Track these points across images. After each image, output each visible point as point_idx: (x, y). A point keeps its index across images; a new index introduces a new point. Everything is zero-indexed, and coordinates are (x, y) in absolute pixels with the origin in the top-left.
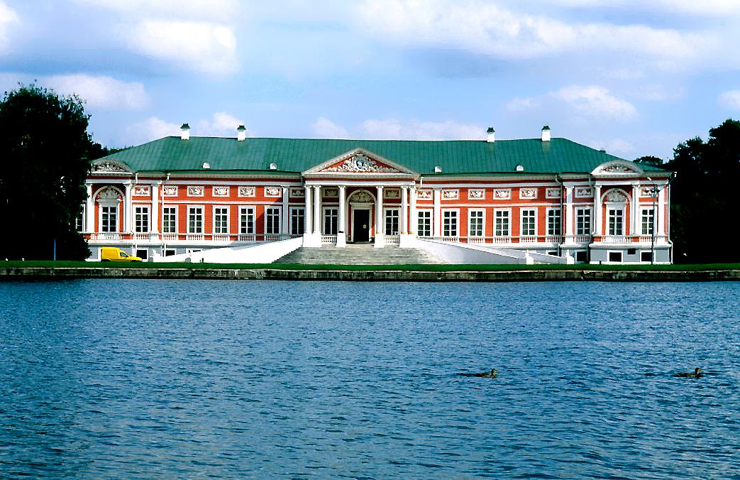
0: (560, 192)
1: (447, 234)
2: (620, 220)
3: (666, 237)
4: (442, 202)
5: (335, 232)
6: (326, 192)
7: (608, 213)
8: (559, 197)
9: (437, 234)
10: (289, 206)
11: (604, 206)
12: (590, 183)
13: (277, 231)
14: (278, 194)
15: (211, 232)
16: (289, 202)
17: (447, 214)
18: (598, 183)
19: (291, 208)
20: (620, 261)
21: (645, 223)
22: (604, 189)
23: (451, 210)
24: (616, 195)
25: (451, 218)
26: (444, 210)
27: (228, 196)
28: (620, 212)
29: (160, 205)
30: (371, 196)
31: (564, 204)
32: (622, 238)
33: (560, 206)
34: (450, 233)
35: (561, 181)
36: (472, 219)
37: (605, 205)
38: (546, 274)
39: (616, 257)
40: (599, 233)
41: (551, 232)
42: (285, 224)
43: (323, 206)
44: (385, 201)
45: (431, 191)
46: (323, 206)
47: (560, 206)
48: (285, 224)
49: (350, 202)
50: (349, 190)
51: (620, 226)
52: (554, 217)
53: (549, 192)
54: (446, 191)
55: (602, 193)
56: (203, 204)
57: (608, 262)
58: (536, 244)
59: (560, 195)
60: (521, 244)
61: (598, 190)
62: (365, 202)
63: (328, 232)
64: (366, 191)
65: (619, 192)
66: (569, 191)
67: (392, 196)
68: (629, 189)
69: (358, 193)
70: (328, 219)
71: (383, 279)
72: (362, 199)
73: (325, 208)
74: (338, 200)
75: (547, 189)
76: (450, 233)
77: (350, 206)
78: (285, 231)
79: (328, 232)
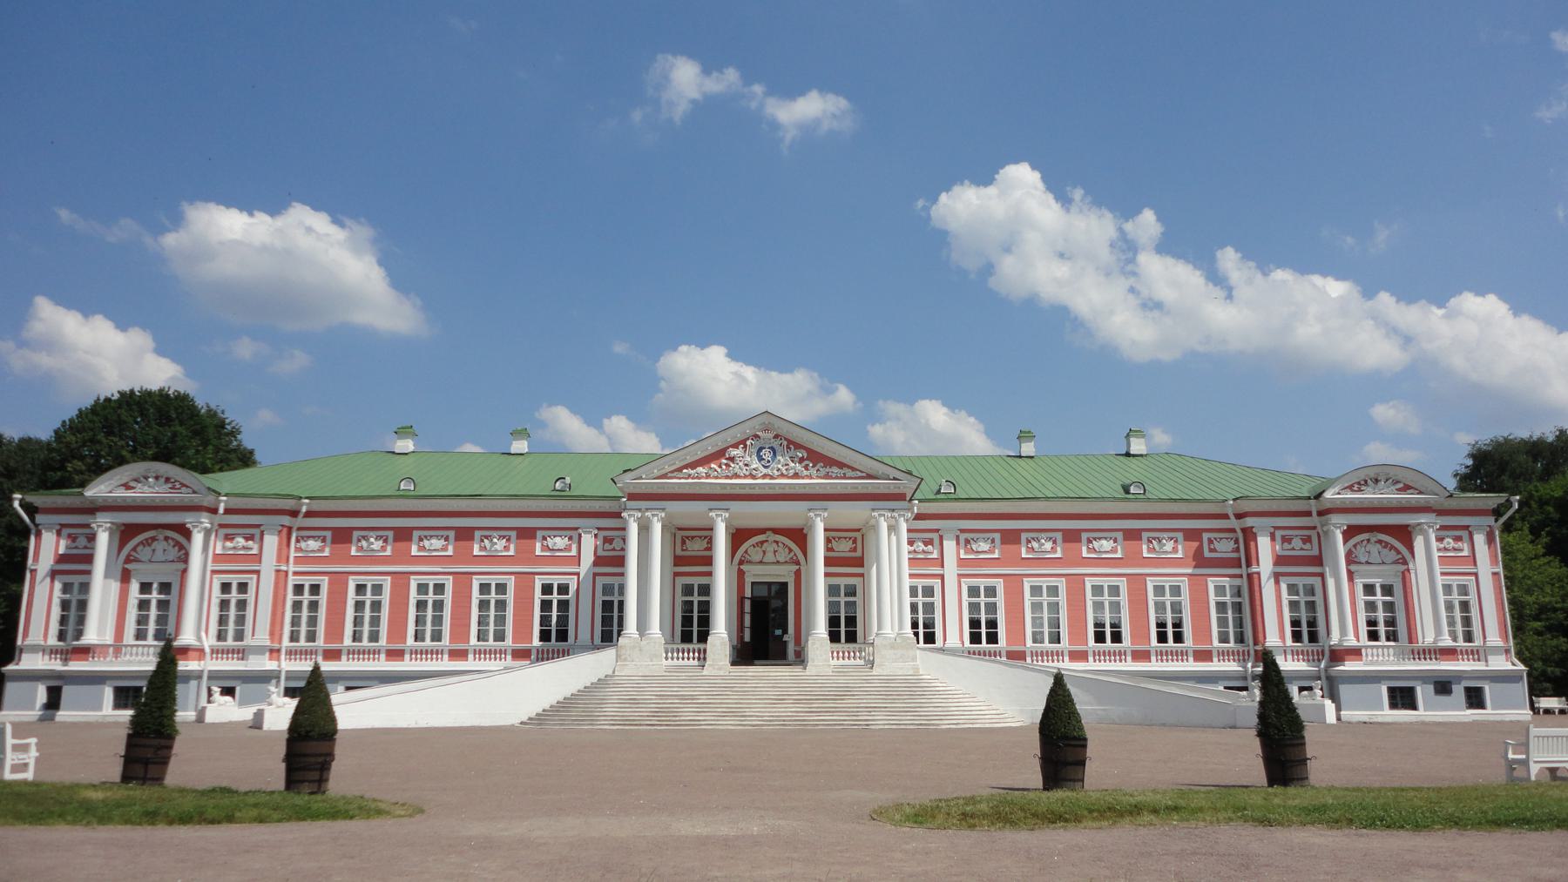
0: (1237, 541)
1: (975, 639)
4: (962, 563)
5: (703, 637)
6: (683, 542)
7: (1360, 589)
8: (1234, 555)
9: (953, 641)
10: (595, 575)
11: (1351, 574)
12: (1314, 520)
14: (568, 549)
15: (404, 639)
17: (973, 592)
18: (1336, 519)
19: (600, 581)
23: (982, 583)
24: (1375, 548)
25: (982, 600)
29: (281, 576)
30: (790, 550)
31: (1254, 569)
33: (1241, 576)
34: (1383, 635)
40: (1351, 641)
41: (1224, 638)
42: (584, 621)
43: (676, 574)
44: (829, 562)
45: (935, 536)
46: (676, 574)
47: (1241, 576)
48: (584, 621)
49: (741, 562)
50: (738, 537)
53: (1210, 541)
54: (969, 536)
55: (1345, 541)
59: (1237, 550)
63: (686, 638)
65: (1380, 542)
67: (843, 548)
68: (1404, 534)
69: (762, 543)
70: (688, 606)
72: (770, 557)
73: (681, 581)
74: (709, 561)
76: (1383, 635)
77: (741, 574)
79: (686, 638)
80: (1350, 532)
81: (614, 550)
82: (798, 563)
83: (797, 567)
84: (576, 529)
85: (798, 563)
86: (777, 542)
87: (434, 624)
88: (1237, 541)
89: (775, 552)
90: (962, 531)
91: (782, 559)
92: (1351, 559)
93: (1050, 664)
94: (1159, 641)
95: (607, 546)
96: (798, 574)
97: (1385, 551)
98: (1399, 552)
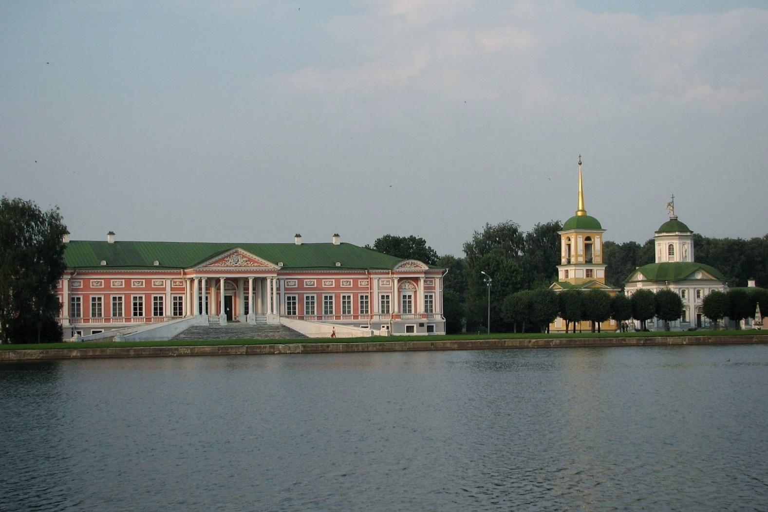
2: (410, 302)
3: (441, 315)
4: (286, 289)
10: (171, 294)
13: (161, 314)
16: (171, 290)
19: (173, 296)
20: (413, 332)
21: (410, 305)
22: (400, 280)
23: (291, 296)
26: (287, 296)
27: (124, 286)
28: (410, 297)
32: (351, 316)
35: (369, 274)
36: (93, 304)
37: (400, 292)
38: (196, 350)
39: (410, 329)
51: (410, 307)
52: (138, 302)
56: (123, 294)
57: (406, 334)
58: (352, 320)
60: (360, 320)
61: (396, 281)
62: (229, 290)
64: (229, 281)
66: (375, 282)
68: (416, 280)
71: (138, 356)
75: (341, 280)
78: (168, 314)
80: (400, 280)
81: (177, 285)
82: (235, 289)
83: (235, 291)
84: (164, 279)
85: (235, 289)
86: (229, 283)
87: (137, 308)
88: (368, 282)
89: (228, 286)
90: (287, 279)
91: (230, 288)
92: (400, 288)
93: (364, 320)
94: (155, 315)
95: (174, 284)
96: (235, 293)
97: (410, 285)
98: (414, 285)
